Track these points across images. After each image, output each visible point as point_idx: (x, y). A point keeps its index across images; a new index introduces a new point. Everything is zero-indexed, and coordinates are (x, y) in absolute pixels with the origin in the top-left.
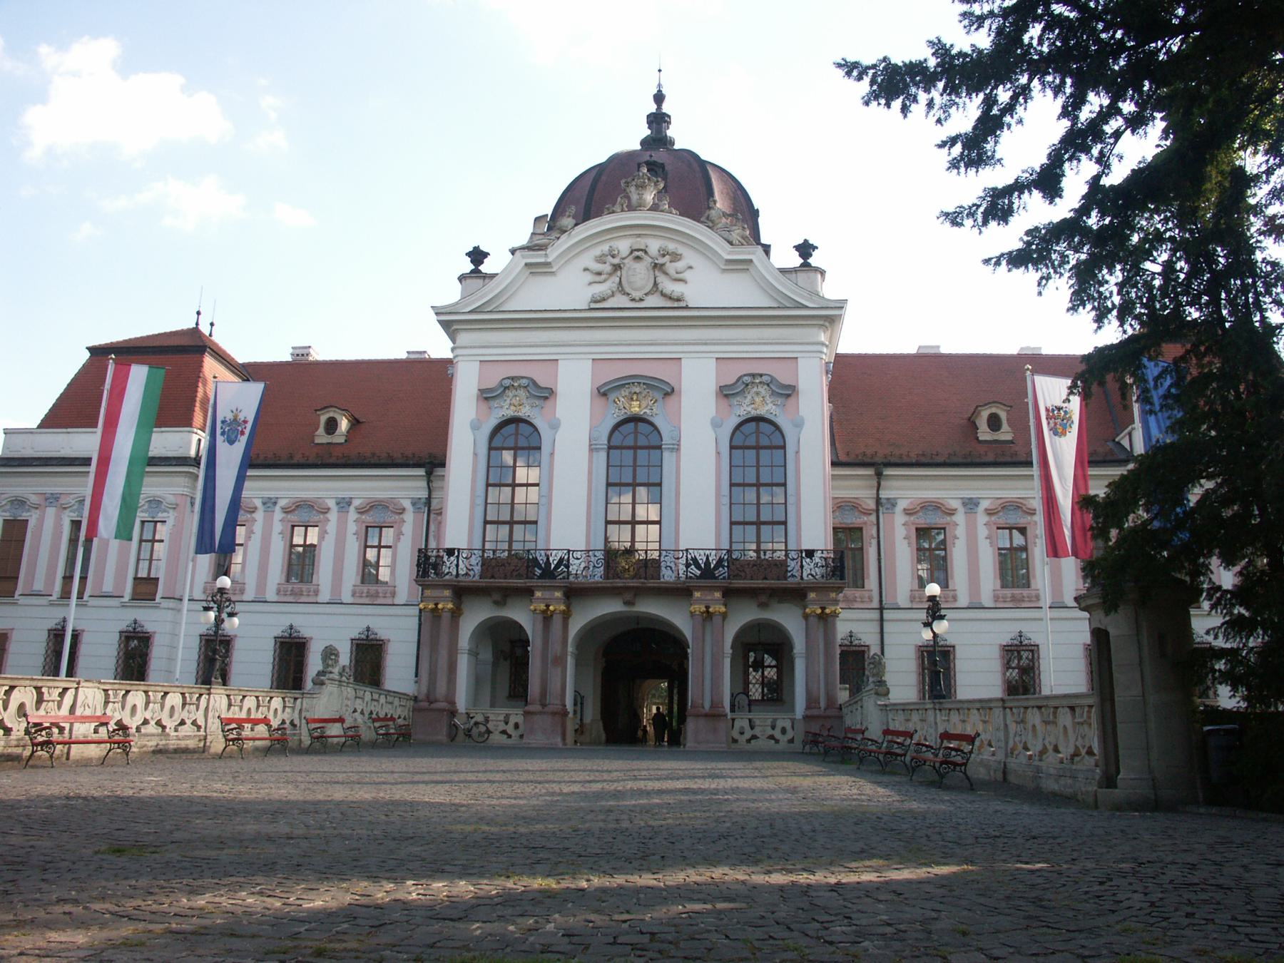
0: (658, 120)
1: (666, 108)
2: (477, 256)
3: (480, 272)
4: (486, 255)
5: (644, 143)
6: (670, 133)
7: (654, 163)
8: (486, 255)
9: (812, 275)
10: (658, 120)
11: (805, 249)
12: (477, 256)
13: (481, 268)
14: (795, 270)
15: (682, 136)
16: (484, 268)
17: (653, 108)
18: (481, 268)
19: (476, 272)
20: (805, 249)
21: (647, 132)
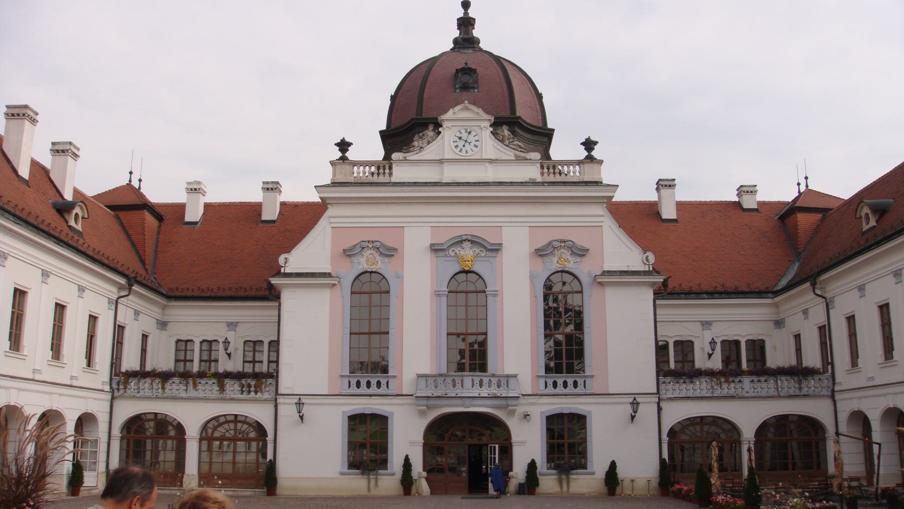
0: (466, 23)
1: (472, 13)
2: (344, 146)
3: (347, 159)
4: (350, 144)
5: (456, 41)
6: (476, 33)
7: (470, 69)
8: (350, 144)
9: (596, 166)
10: (466, 23)
11: (589, 145)
12: (344, 146)
13: (347, 154)
14: (579, 163)
15: (488, 37)
16: (351, 155)
17: (460, 13)
18: (347, 154)
19: (343, 159)
20: (589, 145)
21: (456, 33)
